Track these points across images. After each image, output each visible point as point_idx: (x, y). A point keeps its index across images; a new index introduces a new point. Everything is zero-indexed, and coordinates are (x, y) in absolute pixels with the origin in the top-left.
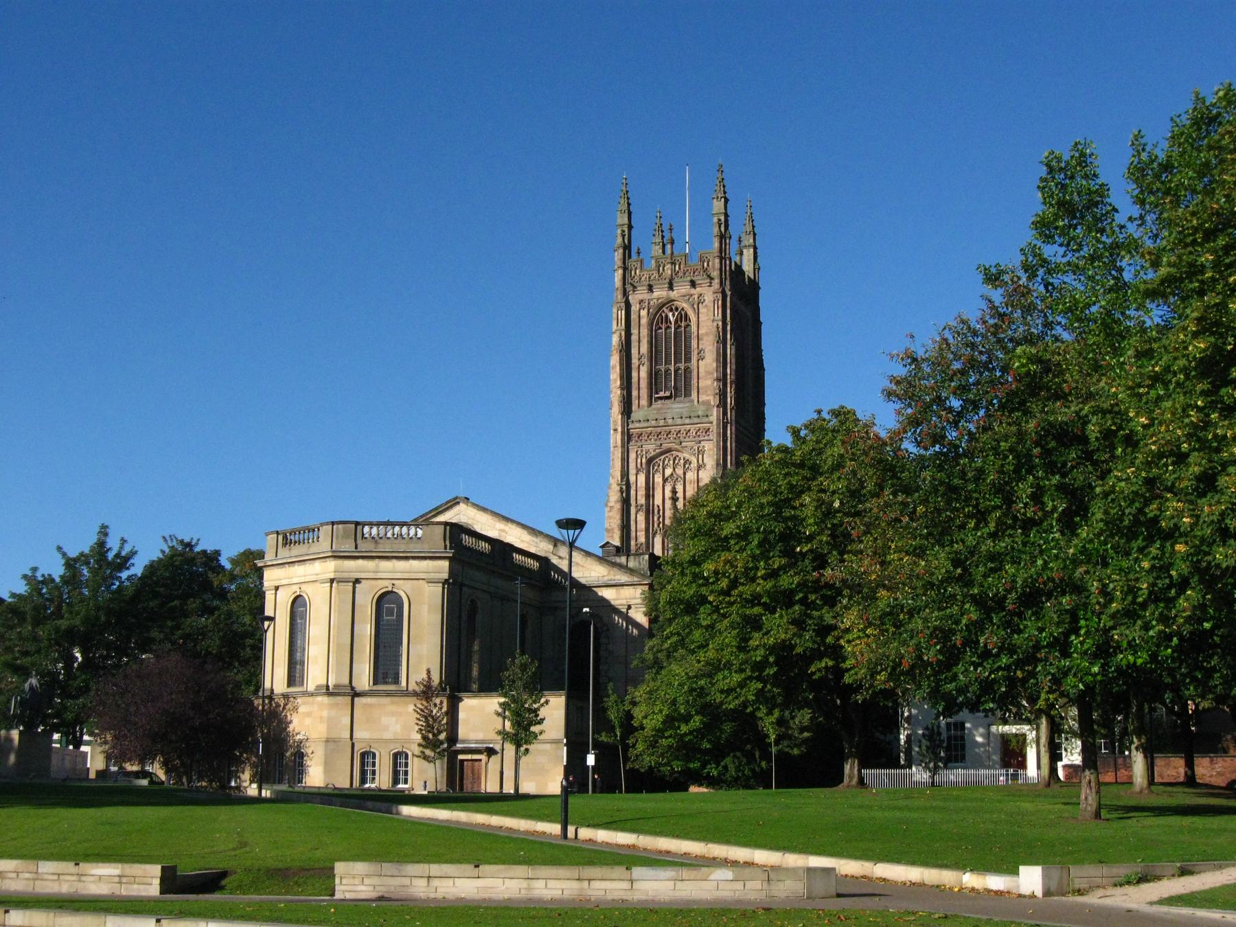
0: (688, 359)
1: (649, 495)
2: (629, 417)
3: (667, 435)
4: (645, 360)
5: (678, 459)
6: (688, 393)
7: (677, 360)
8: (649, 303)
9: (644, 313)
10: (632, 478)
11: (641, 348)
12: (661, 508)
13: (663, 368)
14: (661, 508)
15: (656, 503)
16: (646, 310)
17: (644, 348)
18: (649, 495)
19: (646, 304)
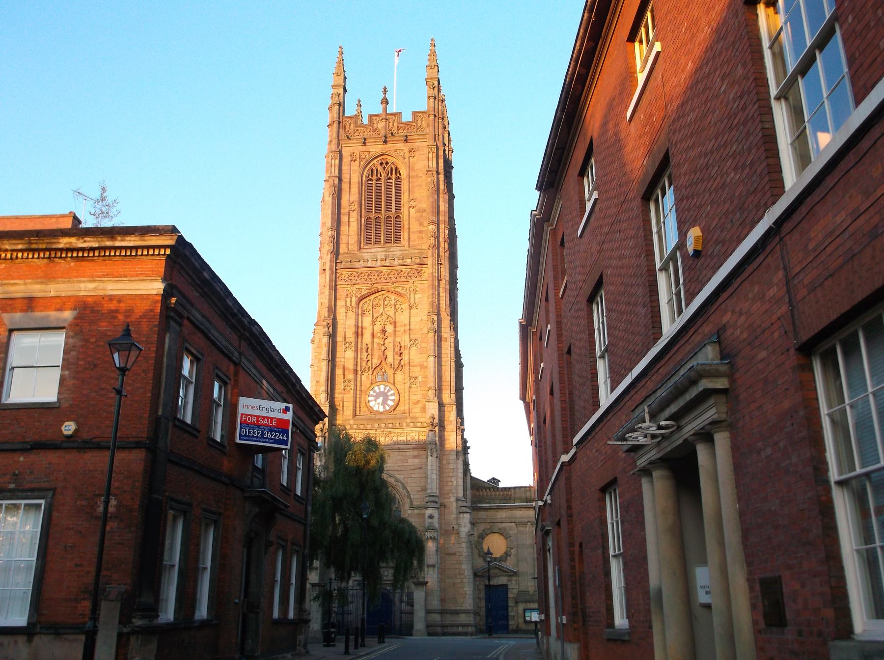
0: (398, 208)
1: (358, 334)
2: (337, 259)
3: (378, 275)
4: (355, 207)
5: (388, 299)
6: (398, 239)
7: (388, 209)
8: (360, 156)
9: (355, 166)
10: (340, 318)
11: (352, 194)
12: (370, 346)
13: (372, 215)
14: (370, 346)
15: (364, 342)
16: (357, 163)
17: (355, 197)
18: (358, 334)
19: (357, 156)
